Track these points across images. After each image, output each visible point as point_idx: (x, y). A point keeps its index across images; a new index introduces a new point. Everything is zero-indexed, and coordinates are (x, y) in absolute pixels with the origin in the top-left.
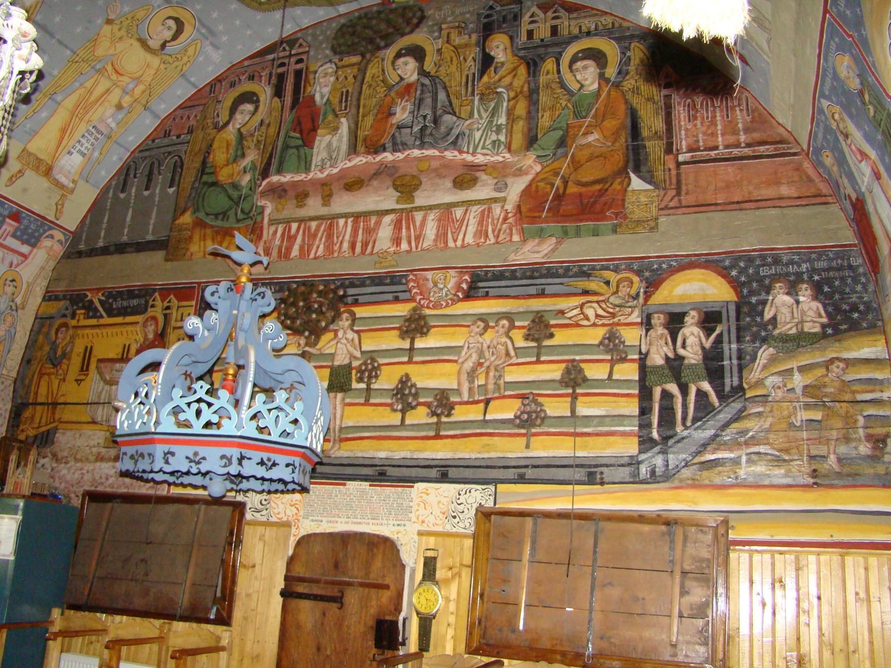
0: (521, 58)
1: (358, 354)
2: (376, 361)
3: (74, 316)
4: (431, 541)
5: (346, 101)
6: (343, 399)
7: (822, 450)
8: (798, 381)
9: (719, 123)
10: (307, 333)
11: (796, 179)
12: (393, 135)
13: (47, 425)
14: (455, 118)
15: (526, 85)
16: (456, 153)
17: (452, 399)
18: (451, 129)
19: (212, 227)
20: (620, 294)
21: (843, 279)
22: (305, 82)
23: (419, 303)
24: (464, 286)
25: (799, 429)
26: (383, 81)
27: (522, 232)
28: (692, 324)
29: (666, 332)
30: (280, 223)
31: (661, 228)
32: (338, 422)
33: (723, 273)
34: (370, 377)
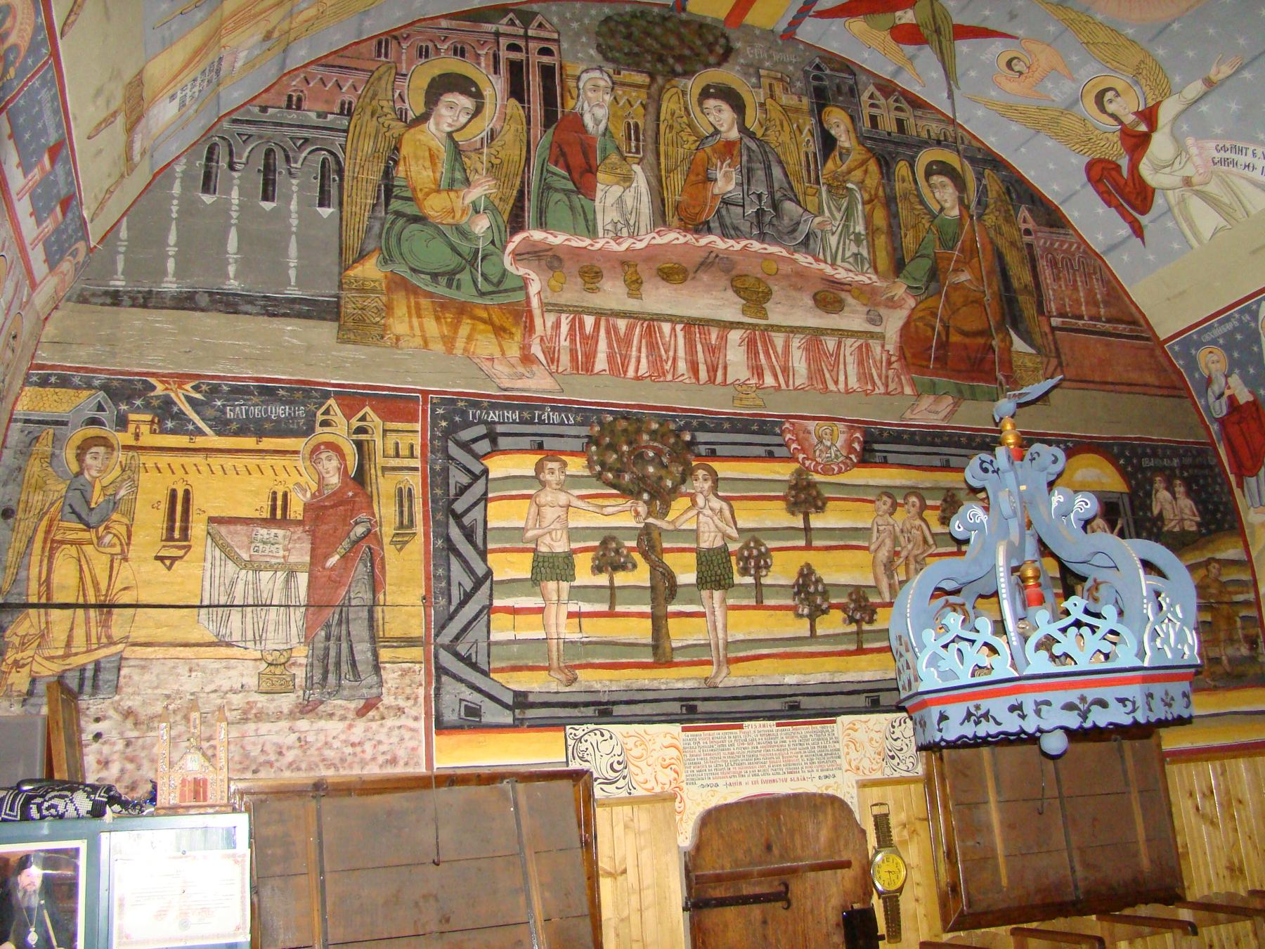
0: (869, 150)
1: (734, 533)
2: (763, 545)
3: (122, 423)
4: (875, 794)
5: (637, 139)
6: (724, 600)
9: (1080, 289)
10: (646, 496)
12: (718, 211)
14: (801, 210)
15: (881, 189)
16: (810, 259)
17: (871, 600)
18: (798, 223)
19: (430, 295)
22: (562, 88)
23: (804, 464)
24: (857, 446)
26: (689, 126)
27: (913, 384)
30: (564, 312)
32: (721, 635)
34: (758, 567)
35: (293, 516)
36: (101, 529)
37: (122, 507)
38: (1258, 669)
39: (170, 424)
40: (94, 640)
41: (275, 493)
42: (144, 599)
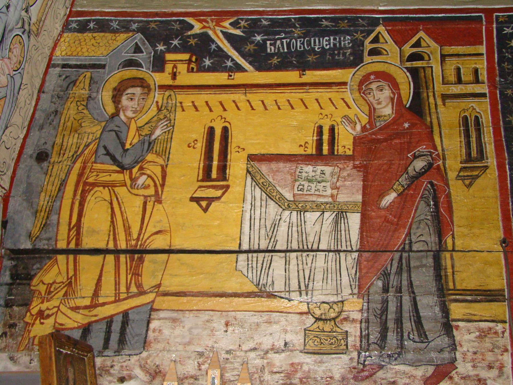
3: (159, 64)
13: (117, 300)
35: (341, 151)
36: (135, 170)
37: (158, 147)
39: (207, 62)
40: (123, 289)
41: (320, 128)
42: (178, 243)
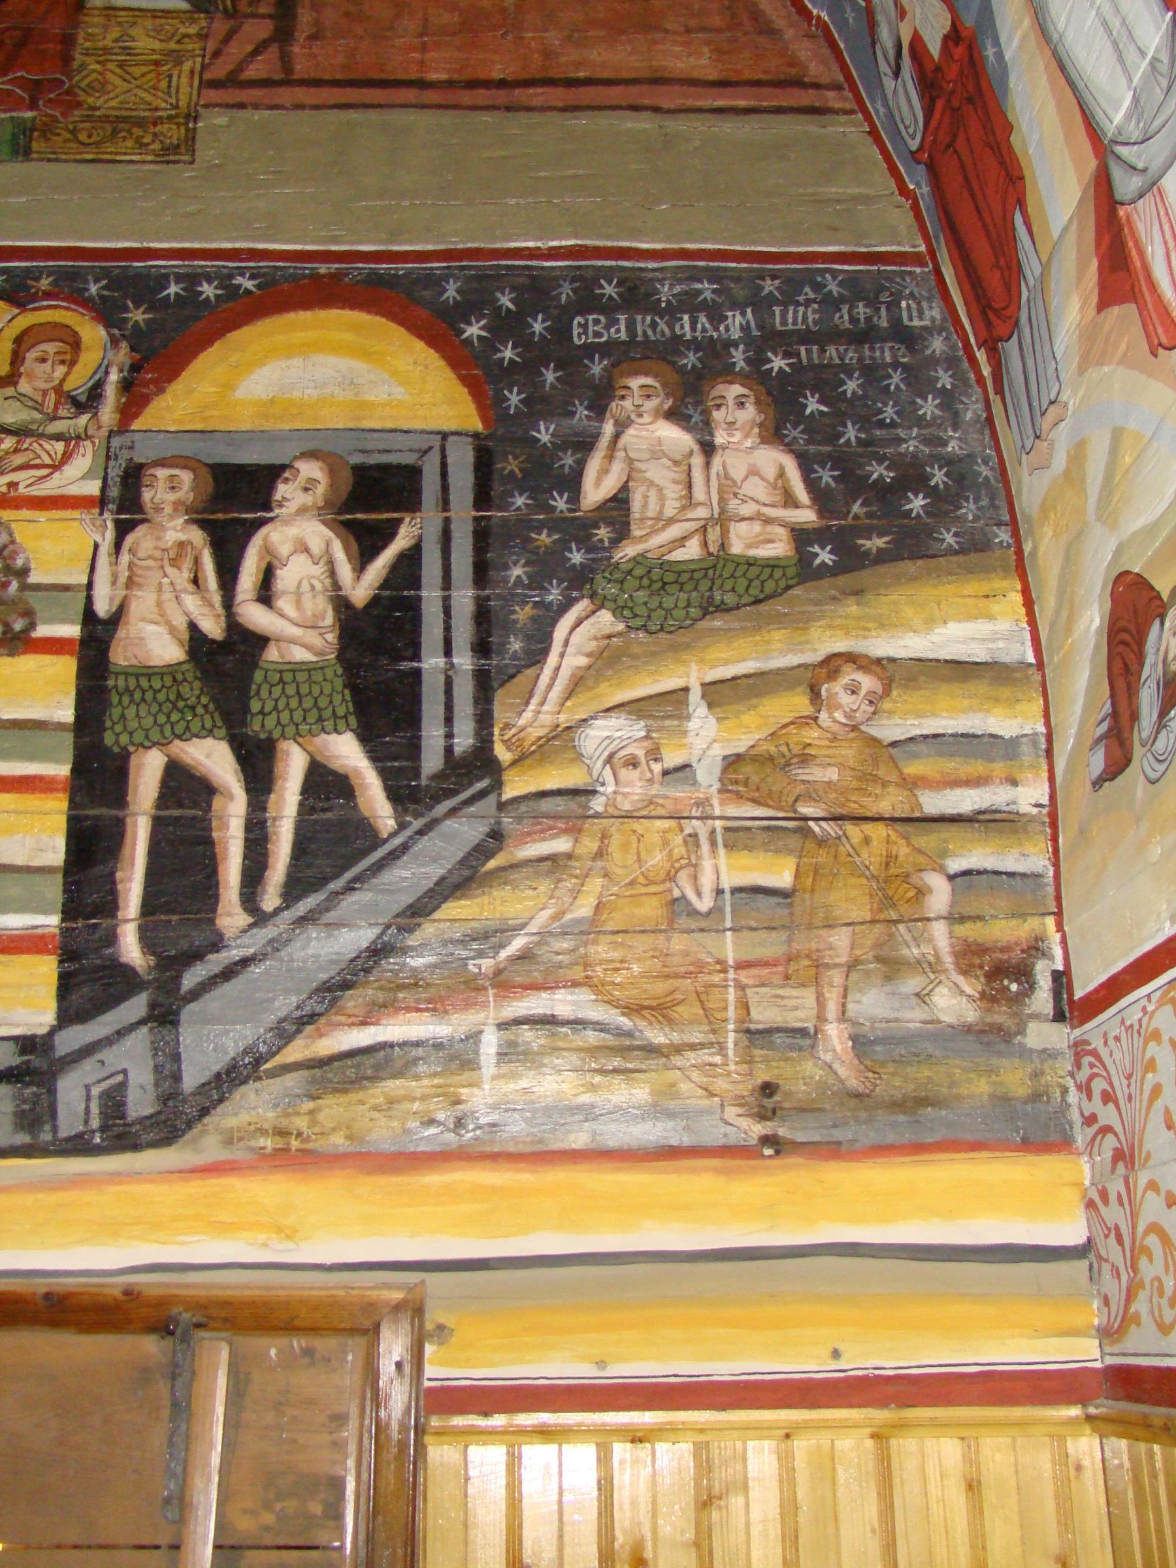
7: (798, 1006)
8: (706, 738)
11: (717, 21)
20: (24, 386)
21: (872, 373)
25: (709, 922)
28: (302, 511)
29: (197, 536)
31: (206, 152)
33: (437, 327)
38: (1015, 1079)
